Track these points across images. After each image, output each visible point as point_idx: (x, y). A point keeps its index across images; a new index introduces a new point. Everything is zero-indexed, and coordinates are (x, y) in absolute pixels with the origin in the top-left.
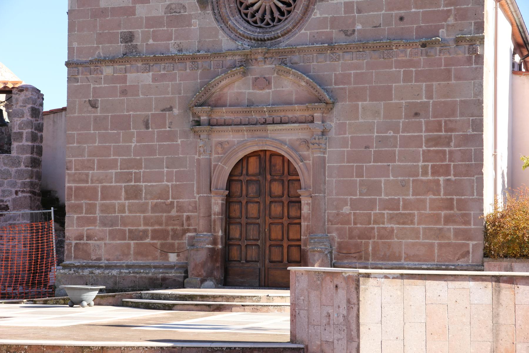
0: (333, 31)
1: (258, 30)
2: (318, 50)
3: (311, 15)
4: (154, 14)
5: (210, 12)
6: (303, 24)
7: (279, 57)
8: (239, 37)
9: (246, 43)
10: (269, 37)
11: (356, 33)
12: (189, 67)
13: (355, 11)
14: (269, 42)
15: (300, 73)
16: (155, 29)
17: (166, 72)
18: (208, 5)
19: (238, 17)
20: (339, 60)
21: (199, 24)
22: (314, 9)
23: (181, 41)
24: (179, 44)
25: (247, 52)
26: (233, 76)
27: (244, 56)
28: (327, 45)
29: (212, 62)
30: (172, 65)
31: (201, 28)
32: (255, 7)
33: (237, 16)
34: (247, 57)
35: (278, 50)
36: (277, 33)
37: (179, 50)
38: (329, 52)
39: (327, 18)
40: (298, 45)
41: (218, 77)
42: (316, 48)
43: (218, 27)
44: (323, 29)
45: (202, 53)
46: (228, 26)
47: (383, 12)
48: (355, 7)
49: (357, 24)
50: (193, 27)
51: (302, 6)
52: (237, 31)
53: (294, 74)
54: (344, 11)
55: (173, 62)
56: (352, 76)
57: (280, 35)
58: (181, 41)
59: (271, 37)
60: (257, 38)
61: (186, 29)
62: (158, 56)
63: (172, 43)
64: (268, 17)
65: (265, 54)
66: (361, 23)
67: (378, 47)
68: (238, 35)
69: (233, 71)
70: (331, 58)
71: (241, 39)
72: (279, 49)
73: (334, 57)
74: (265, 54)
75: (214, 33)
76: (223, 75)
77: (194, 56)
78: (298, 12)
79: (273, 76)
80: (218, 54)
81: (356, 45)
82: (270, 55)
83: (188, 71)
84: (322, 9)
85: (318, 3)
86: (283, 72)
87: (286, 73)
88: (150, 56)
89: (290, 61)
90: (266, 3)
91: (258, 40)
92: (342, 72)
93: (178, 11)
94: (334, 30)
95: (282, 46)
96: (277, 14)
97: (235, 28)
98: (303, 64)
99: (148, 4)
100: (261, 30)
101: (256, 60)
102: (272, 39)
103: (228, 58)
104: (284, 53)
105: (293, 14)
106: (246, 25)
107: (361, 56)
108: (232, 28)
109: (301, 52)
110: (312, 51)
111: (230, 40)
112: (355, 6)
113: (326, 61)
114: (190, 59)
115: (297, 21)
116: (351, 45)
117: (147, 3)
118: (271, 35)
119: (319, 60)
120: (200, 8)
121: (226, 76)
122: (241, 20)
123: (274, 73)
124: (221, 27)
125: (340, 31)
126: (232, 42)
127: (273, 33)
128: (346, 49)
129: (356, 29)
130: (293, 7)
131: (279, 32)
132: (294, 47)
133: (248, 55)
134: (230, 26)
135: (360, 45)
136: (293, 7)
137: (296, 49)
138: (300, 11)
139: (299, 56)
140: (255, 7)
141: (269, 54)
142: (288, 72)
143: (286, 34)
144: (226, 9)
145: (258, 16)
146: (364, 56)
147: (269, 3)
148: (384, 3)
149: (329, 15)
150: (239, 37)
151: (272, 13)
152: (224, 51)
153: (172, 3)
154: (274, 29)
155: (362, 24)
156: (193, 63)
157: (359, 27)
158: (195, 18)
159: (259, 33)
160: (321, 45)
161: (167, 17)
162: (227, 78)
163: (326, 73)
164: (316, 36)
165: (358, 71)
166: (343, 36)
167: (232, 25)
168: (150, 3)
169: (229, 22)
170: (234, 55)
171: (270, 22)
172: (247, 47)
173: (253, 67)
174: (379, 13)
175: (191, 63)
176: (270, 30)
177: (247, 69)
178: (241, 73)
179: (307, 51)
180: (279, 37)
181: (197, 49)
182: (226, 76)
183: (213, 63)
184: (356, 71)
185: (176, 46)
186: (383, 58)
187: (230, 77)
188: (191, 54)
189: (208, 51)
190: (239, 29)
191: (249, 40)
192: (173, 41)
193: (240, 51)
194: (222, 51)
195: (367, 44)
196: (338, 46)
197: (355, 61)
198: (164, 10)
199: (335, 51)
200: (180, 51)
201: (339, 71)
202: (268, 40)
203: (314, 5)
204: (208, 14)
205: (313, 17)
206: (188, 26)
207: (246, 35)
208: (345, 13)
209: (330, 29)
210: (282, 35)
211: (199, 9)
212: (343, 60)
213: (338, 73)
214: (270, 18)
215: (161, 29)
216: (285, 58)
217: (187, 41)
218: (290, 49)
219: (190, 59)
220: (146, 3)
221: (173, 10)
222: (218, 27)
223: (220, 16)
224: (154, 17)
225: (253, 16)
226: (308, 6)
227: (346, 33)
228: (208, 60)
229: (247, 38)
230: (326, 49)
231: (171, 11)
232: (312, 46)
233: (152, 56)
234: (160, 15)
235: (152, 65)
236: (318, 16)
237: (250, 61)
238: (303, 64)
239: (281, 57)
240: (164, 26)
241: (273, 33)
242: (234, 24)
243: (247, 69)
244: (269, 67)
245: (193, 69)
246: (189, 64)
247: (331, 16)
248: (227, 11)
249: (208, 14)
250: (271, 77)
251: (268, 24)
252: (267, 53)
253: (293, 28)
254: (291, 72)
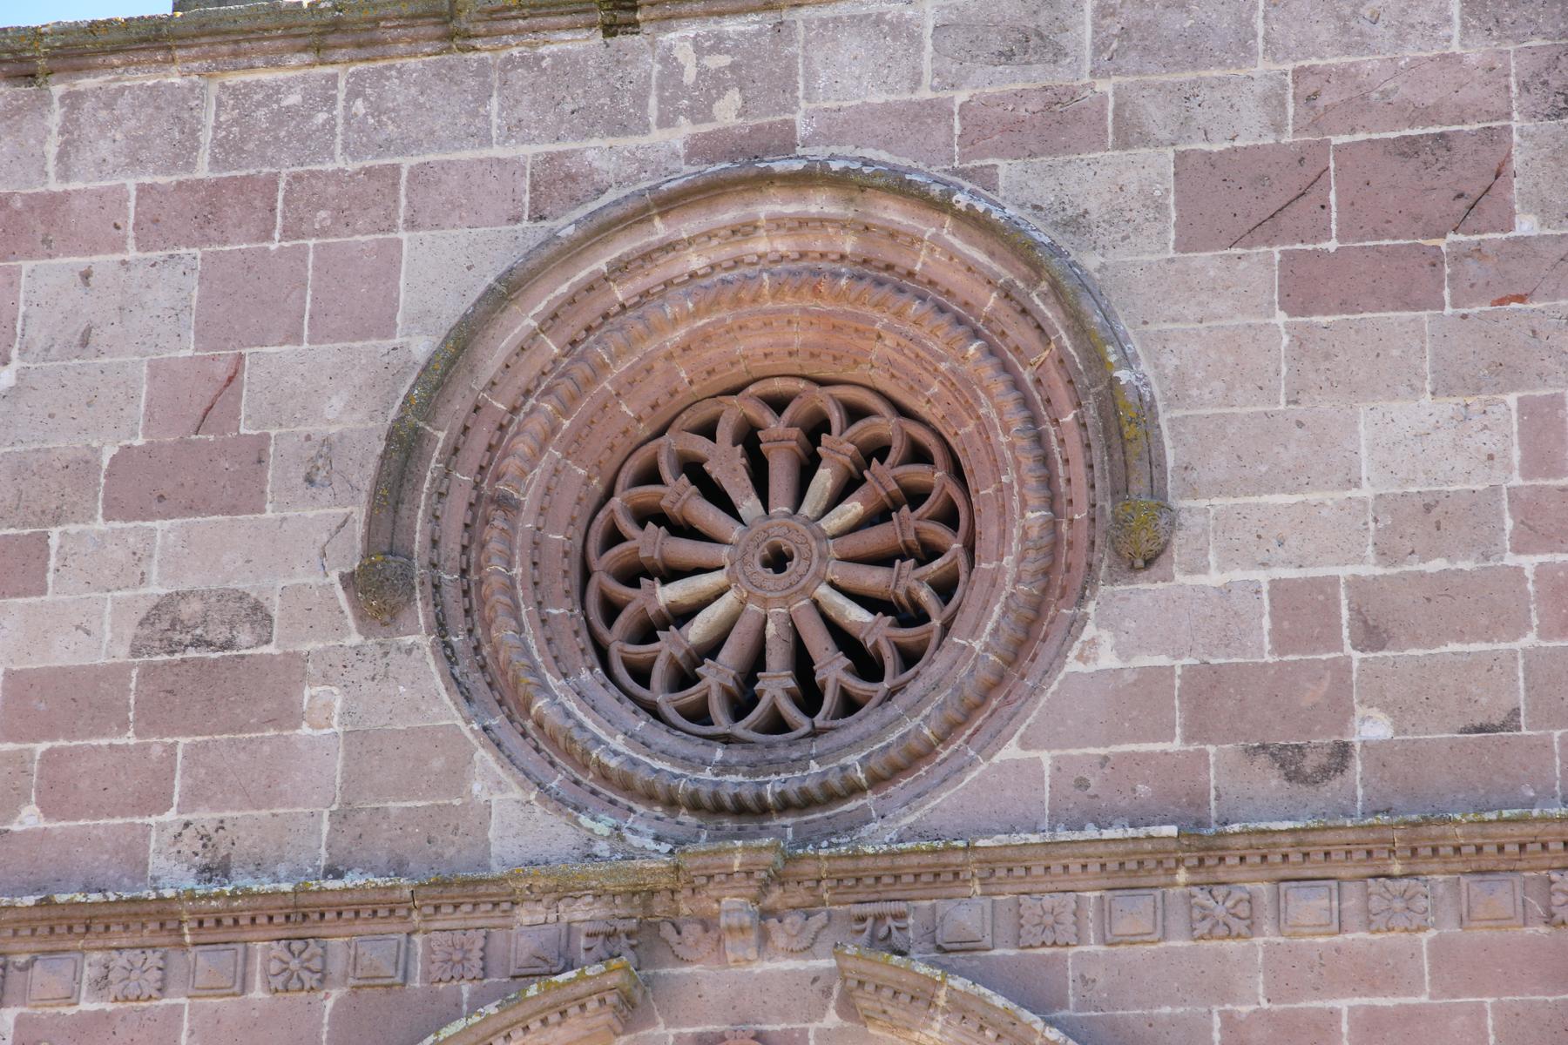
0: (1204, 755)
1: (719, 754)
2: (1112, 866)
3: (1061, 655)
4: (65, 652)
5: (418, 637)
6: (1006, 711)
7: (858, 910)
8: (594, 792)
9: (640, 826)
10: (792, 789)
11: (1357, 766)
12: (265, 970)
13: (1346, 632)
14: (788, 821)
15: (999, 1001)
16: (61, 743)
17: (109, 1007)
18: (411, 599)
19: (590, 676)
20: (1253, 927)
21: (347, 713)
22: (1077, 624)
23: (228, 814)
24: (210, 829)
25: (653, 873)
26: (554, 1018)
27: (630, 901)
28: (1171, 830)
29: (418, 939)
30: (153, 958)
31: (359, 740)
32: (698, 630)
33: (585, 675)
34: (646, 905)
35: (848, 865)
36: (844, 769)
37: (206, 869)
38: (1182, 876)
39: (1166, 673)
40: (989, 833)
41: (460, 1025)
42: (1101, 848)
43: (466, 730)
44: (1139, 740)
45: (352, 880)
46: (529, 724)
47: (1530, 640)
48: (1345, 614)
49: (1360, 711)
50: (305, 730)
51: (997, 609)
52: (586, 753)
53: (961, 1008)
54: (1271, 632)
55: (164, 939)
56: (1345, 1028)
57: (861, 775)
58: (228, 814)
59: (803, 792)
60: (715, 796)
61: (262, 741)
62: (72, 904)
63: (163, 827)
64: (776, 685)
65: (765, 887)
66: (1386, 708)
67: (1512, 849)
68: (588, 780)
69: (559, 986)
70: (1197, 914)
71: (612, 802)
72: (856, 856)
73: (1220, 912)
74: (765, 887)
75: (437, 764)
76: (491, 1009)
77: (304, 899)
78: (977, 645)
79: (812, 1027)
80: (464, 883)
81: (1363, 835)
82: (799, 896)
83: (258, 993)
84: (1129, 624)
85: (1104, 590)
86: (887, 993)
87: (904, 998)
88: (18, 902)
89: (931, 932)
90: (765, 602)
91: (718, 809)
92: (1275, 1007)
93: (219, 634)
94: (1211, 749)
95: (877, 838)
96: (832, 669)
97: (575, 733)
98: (1012, 952)
99: (33, 600)
100: (736, 755)
101: (707, 924)
102: (807, 802)
103: (524, 915)
104: (886, 880)
105: (935, 667)
106: (641, 724)
107: (1398, 905)
108: (553, 740)
109: (1001, 873)
110: (1075, 868)
111: (538, 808)
112: (1344, 602)
113: (1164, 938)
114: (279, 919)
115: (971, 695)
116: (1330, 836)
117: (26, 593)
118: (803, 779)
119: (1123, 927)
120: (361, 618)
121: (511, 1016)
122: (608, 698)
123: (825, 1008)
124: (485, 729)
125: (1251, 752)
126: (554, 819)
127: (814, 767)
128: (1295, 857)
129: (1356, 740)
130: (936, 622)
131: (852, 759)
132: (961, 844)
133: (652, 893)
134: (539, 725)
135: (1388, 834)
136: (886, 685)
137: (972, 857)
138: (985, 637)
139: (987, 902)
140: (698, 630)
141: (792, 886)
142: (922, 997)
143: (898, 771)
144: (520, 629)
145: (717, 677)
146: (1421, 903)
147: (786, 601)
148: (1530, 587)
149: (1179, 656)
150: (594, 792)
151: (802, 663)
152: (497, 871)
153: (184, 588)
154: (816, 747)
155: (1397, 710)
156: (297, 946)
157: (1371, 728)
158: (326, 679)
159: (725, 767)
160: (1131, 832)
161: (148, 672)
162: (517, 1033)
163: (1167, 1010)
164: (1092, 781)
165: (1380, 1001)
166: (1274, 782)
167: (553, 718)
168: (42, 591)
169: (540, 704)
170: (563, 891)
171: (790, 711)
172: (651, 845)
173: (687, 970)
174: (1503, 646)
175: (278, 949)
176: (795, 755)
177: (648, 982)
178: (611, 999)
179: (1038, 871)
180: (855, 790)
181: (322, 863)
182: (511, 1016)
183: (427, 944)
184: (1365, 1001)
185: (190, 842)
186: (1550, 919)
187: (535, 1025)
188: (286, 887)
189: (399, 867)
190: (599, 741)
191: (658, 810)
192: (171, 816)
193: (605, 867)
194: (488, 868)
195: (1435, 831)
196: (1242, 842)
197: (1357, 937)
198: (129, 631)
199: (1221, 874)
200: (215, 870)
201: (1254, 1001)
202: (785, 805)
203: (1082, 600)
204: (409, 651)
205: (1072, 665)
206: (272, 722)
207: (641, 775)
208: (1280, 646)
209: (1188, 739)
210: (877, 781)
211: (351, 622)
212: (1280, 933)
213: (1245, 1009)
214: (788, 692)
215: (104, 742)
216: (895, 917)
217: (265, 812)
218: (930, 859)
219: (279, 919)
220: (18, 595)
221: (187, 629)
222: (470, 731)
223: (483, 668)
224: (64, 672)
225: (684, 678)
226: (1038, 609)
227: (1289, 762)
228: (394, 925)
229: (650, 797)
230: (1162, 858)
231: (177, 637)
232: (1076, 836)
233: (30, 900)
234: (102, 660)
235: (22, 959)
236: (1107, 660)
237: (667, 931)
238: (1012, 952)
239: (868, 909)
240: (123, 726)
241: (814, 767)
242: (568, 715)
243: (648, 982)
244: (793, 972)
245: (294, 984)
246: (263, 952)
247: (1187, 661)
248: (524, 642)
249: (409, 651)
250: (804, 1032)
251: (777, 724)
252: (778, 878)
253: (943, 739)
254: (942, 993)
